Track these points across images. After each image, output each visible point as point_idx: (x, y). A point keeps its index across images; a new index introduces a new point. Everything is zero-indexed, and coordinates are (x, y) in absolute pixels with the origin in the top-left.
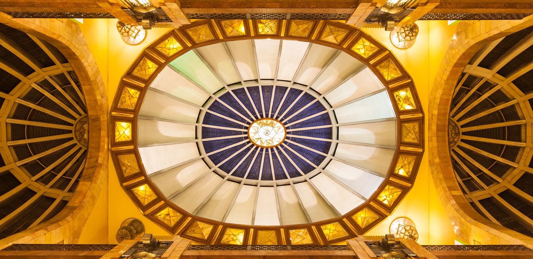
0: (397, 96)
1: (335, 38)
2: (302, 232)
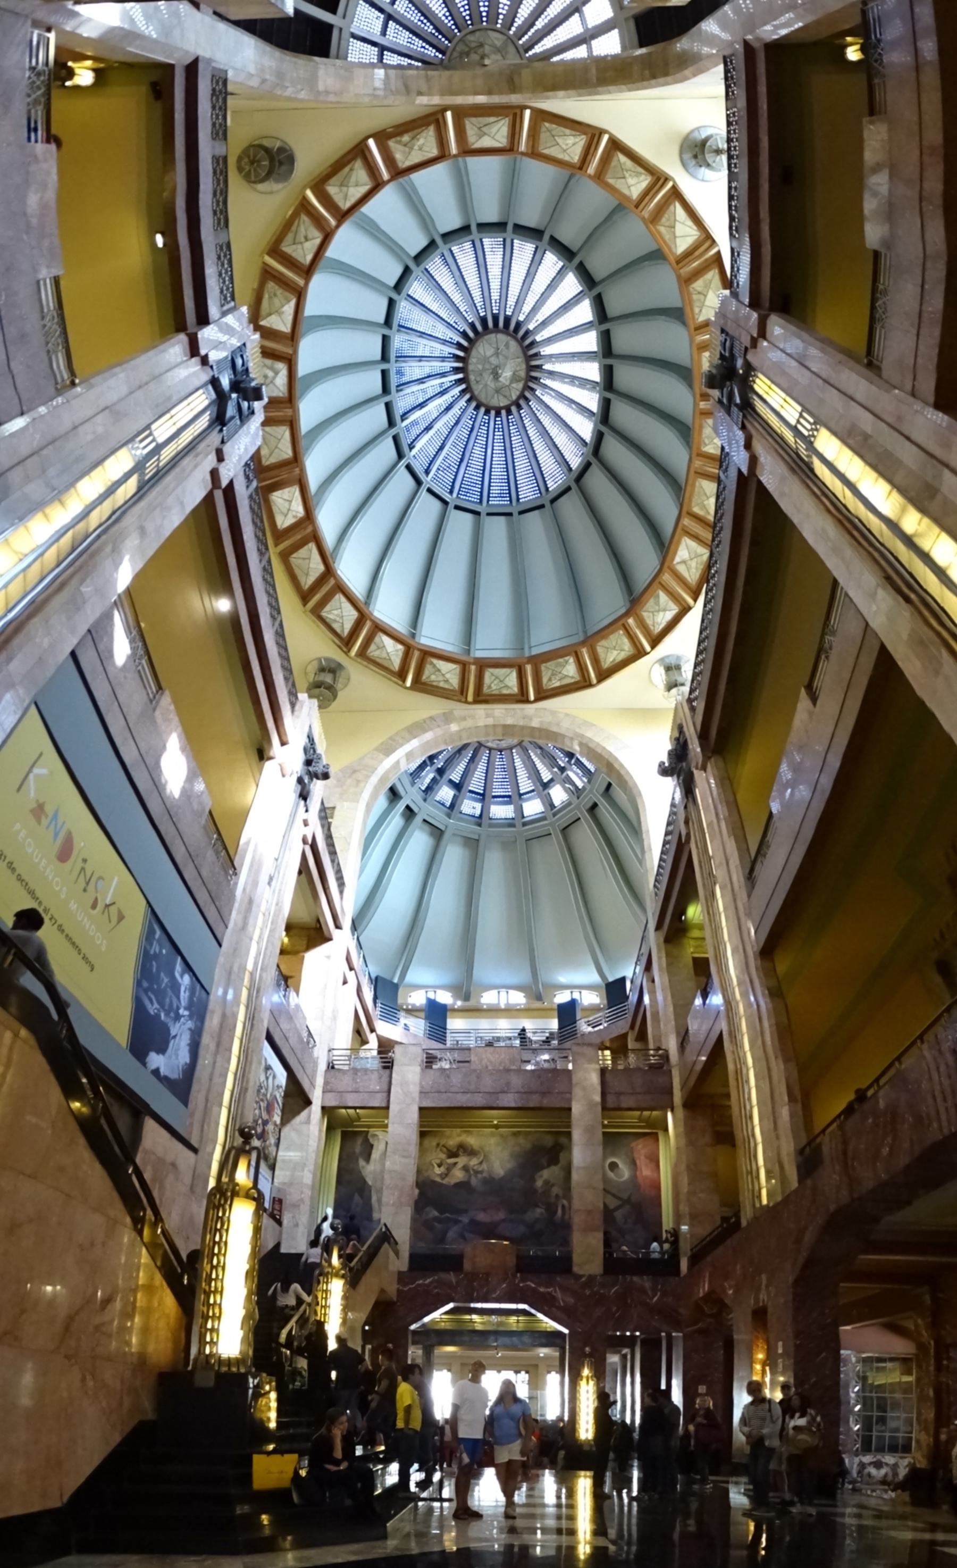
0: (567, 662)
1: (684, 562)
2: (298, 509)
